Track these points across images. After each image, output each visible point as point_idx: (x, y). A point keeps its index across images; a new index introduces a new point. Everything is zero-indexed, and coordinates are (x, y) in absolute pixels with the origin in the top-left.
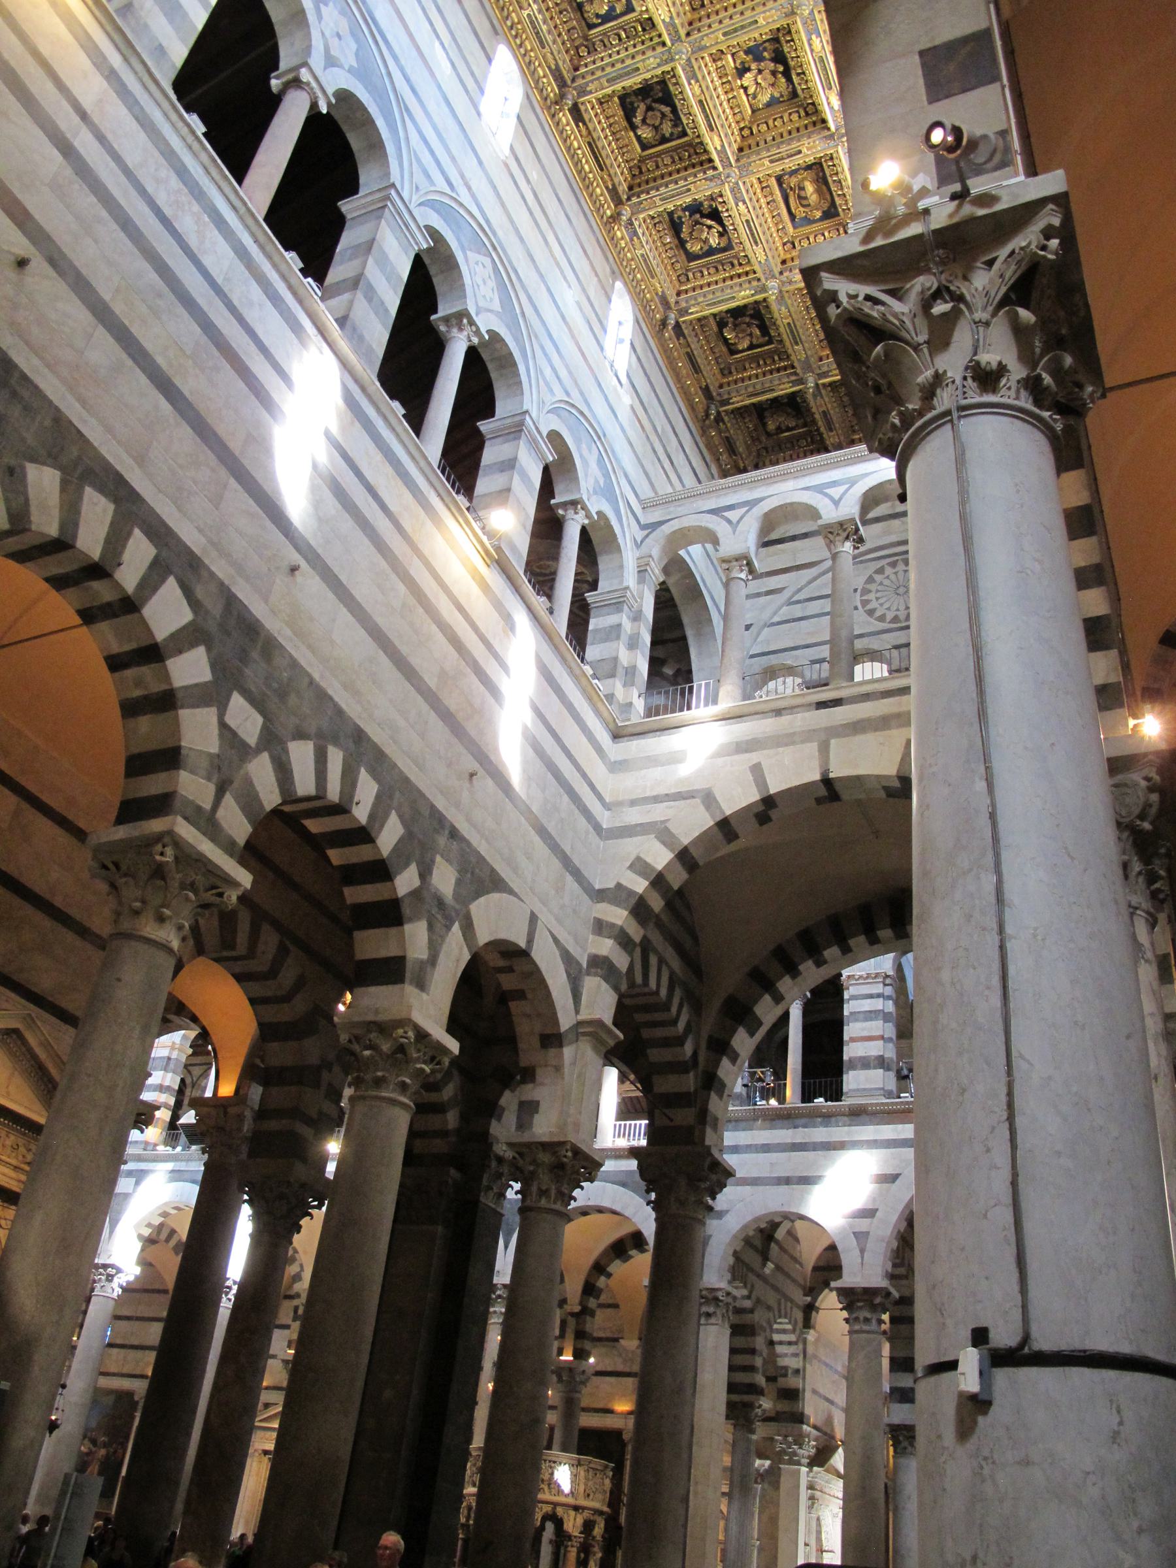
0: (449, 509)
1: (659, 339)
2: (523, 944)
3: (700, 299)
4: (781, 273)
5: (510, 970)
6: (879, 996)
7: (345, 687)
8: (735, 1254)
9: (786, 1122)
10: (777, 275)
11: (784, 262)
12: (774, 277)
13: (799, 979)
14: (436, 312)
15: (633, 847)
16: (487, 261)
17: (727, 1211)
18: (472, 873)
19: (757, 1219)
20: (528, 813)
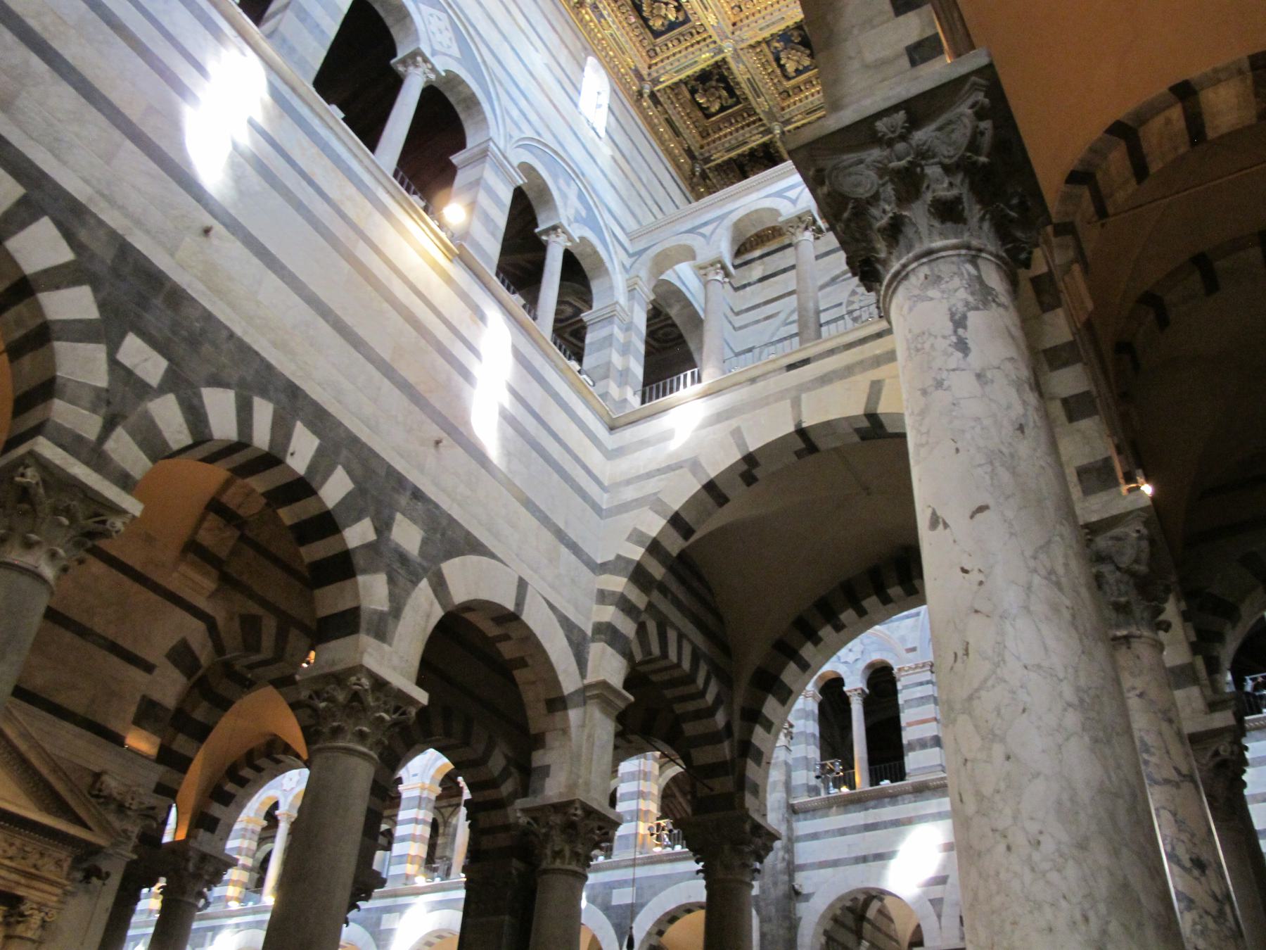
0: (402, 206)
1: (638, 108)
2: (511, 606)
3: (668, 68)
4: (733, 33)
5: (506, 637)
6: (928, 682)
7: (274, 344)
8: (826, 933)
9: (858, 806)
10: (730, 35)
11: (734, 24)
12: (727, 38)
13: (821, 645)
14: (395, 55)
15: (629, 521)
16: (443, 16)
17: (813, 893)
18: (443, 535)
19: (840, 899)
20: (509, 485)
